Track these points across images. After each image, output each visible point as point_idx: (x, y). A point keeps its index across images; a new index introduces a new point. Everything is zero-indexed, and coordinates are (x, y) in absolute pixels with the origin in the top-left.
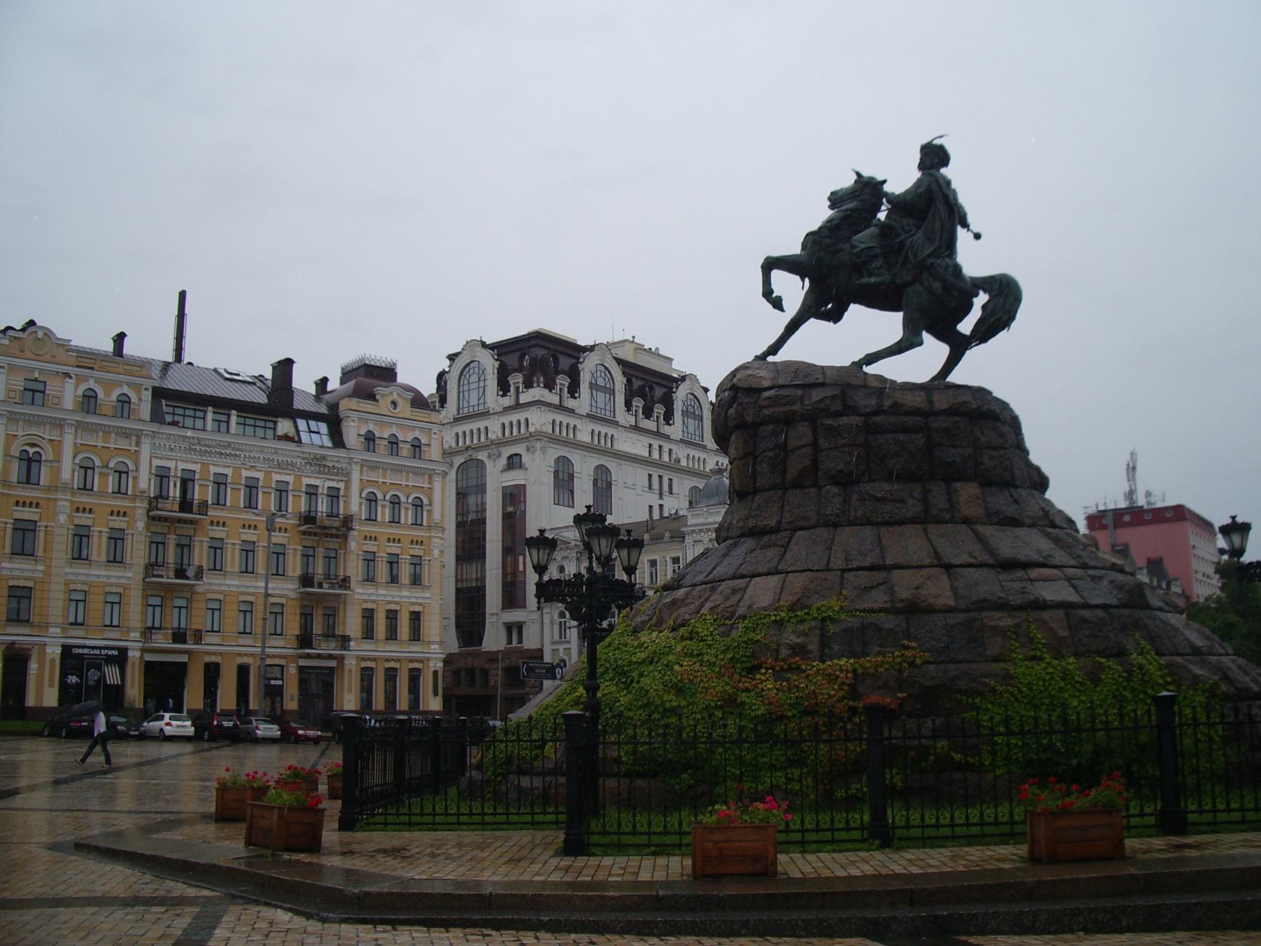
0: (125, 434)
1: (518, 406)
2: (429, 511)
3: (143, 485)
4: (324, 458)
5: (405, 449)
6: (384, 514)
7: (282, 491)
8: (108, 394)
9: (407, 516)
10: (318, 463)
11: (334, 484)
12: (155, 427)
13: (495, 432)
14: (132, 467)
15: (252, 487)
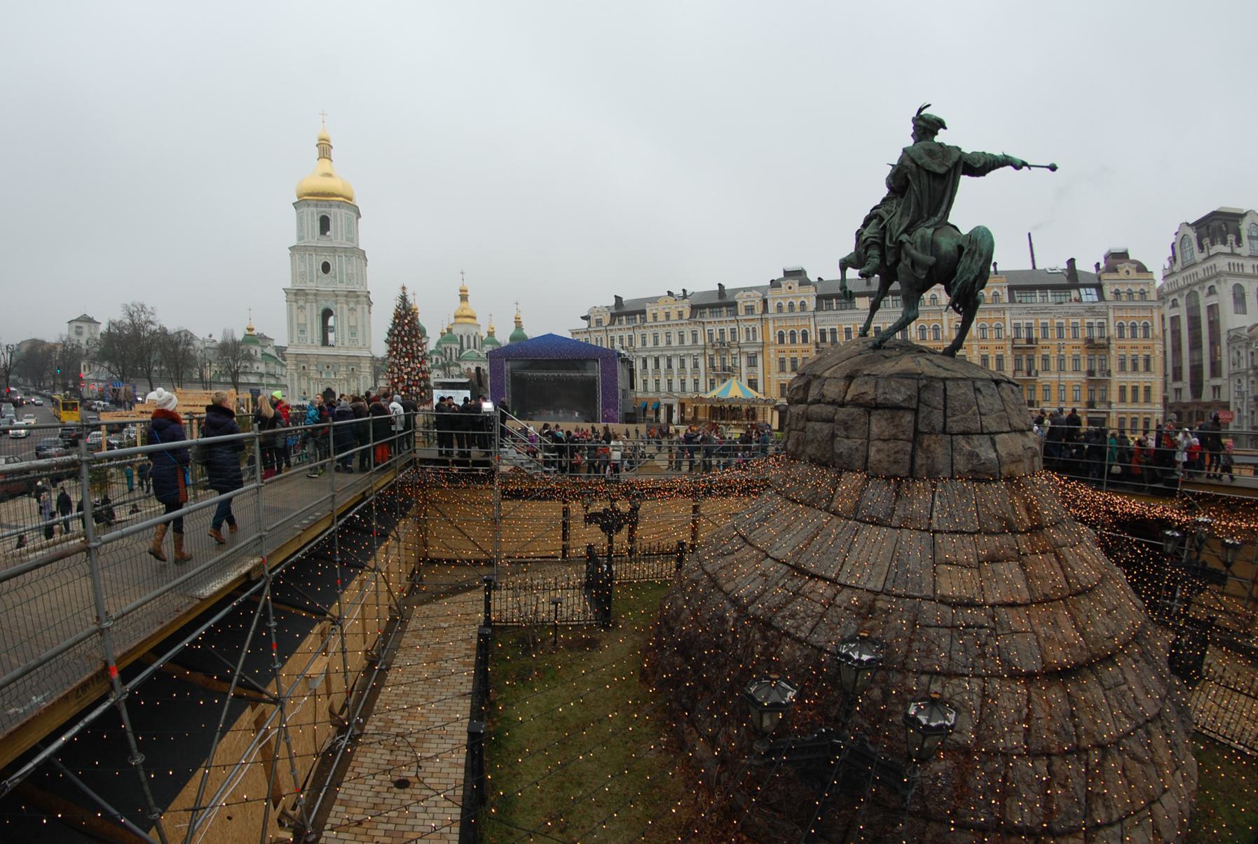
0: (998, 310)
1: (1210, 257)
2: (1152, 330)
3: (1008, 333)
4: (1094, 307)
5: (1137, 296)
6: (1127, 333)
7: (1075, 328)
8: (988, 293)
9: (1140, 333)
10: (1091, 310)
11: (1101, 321)
12: (1010, 305)
13: (1201, 275)
14: (1003, 325)
15: (1060, 327)
